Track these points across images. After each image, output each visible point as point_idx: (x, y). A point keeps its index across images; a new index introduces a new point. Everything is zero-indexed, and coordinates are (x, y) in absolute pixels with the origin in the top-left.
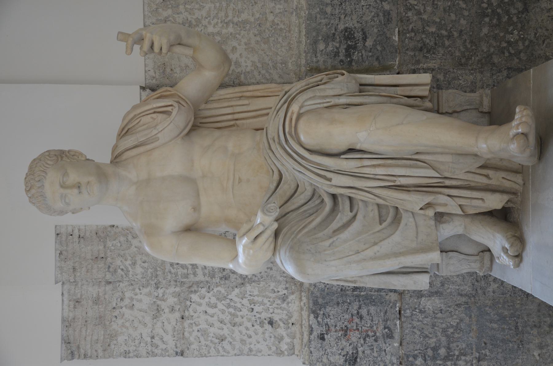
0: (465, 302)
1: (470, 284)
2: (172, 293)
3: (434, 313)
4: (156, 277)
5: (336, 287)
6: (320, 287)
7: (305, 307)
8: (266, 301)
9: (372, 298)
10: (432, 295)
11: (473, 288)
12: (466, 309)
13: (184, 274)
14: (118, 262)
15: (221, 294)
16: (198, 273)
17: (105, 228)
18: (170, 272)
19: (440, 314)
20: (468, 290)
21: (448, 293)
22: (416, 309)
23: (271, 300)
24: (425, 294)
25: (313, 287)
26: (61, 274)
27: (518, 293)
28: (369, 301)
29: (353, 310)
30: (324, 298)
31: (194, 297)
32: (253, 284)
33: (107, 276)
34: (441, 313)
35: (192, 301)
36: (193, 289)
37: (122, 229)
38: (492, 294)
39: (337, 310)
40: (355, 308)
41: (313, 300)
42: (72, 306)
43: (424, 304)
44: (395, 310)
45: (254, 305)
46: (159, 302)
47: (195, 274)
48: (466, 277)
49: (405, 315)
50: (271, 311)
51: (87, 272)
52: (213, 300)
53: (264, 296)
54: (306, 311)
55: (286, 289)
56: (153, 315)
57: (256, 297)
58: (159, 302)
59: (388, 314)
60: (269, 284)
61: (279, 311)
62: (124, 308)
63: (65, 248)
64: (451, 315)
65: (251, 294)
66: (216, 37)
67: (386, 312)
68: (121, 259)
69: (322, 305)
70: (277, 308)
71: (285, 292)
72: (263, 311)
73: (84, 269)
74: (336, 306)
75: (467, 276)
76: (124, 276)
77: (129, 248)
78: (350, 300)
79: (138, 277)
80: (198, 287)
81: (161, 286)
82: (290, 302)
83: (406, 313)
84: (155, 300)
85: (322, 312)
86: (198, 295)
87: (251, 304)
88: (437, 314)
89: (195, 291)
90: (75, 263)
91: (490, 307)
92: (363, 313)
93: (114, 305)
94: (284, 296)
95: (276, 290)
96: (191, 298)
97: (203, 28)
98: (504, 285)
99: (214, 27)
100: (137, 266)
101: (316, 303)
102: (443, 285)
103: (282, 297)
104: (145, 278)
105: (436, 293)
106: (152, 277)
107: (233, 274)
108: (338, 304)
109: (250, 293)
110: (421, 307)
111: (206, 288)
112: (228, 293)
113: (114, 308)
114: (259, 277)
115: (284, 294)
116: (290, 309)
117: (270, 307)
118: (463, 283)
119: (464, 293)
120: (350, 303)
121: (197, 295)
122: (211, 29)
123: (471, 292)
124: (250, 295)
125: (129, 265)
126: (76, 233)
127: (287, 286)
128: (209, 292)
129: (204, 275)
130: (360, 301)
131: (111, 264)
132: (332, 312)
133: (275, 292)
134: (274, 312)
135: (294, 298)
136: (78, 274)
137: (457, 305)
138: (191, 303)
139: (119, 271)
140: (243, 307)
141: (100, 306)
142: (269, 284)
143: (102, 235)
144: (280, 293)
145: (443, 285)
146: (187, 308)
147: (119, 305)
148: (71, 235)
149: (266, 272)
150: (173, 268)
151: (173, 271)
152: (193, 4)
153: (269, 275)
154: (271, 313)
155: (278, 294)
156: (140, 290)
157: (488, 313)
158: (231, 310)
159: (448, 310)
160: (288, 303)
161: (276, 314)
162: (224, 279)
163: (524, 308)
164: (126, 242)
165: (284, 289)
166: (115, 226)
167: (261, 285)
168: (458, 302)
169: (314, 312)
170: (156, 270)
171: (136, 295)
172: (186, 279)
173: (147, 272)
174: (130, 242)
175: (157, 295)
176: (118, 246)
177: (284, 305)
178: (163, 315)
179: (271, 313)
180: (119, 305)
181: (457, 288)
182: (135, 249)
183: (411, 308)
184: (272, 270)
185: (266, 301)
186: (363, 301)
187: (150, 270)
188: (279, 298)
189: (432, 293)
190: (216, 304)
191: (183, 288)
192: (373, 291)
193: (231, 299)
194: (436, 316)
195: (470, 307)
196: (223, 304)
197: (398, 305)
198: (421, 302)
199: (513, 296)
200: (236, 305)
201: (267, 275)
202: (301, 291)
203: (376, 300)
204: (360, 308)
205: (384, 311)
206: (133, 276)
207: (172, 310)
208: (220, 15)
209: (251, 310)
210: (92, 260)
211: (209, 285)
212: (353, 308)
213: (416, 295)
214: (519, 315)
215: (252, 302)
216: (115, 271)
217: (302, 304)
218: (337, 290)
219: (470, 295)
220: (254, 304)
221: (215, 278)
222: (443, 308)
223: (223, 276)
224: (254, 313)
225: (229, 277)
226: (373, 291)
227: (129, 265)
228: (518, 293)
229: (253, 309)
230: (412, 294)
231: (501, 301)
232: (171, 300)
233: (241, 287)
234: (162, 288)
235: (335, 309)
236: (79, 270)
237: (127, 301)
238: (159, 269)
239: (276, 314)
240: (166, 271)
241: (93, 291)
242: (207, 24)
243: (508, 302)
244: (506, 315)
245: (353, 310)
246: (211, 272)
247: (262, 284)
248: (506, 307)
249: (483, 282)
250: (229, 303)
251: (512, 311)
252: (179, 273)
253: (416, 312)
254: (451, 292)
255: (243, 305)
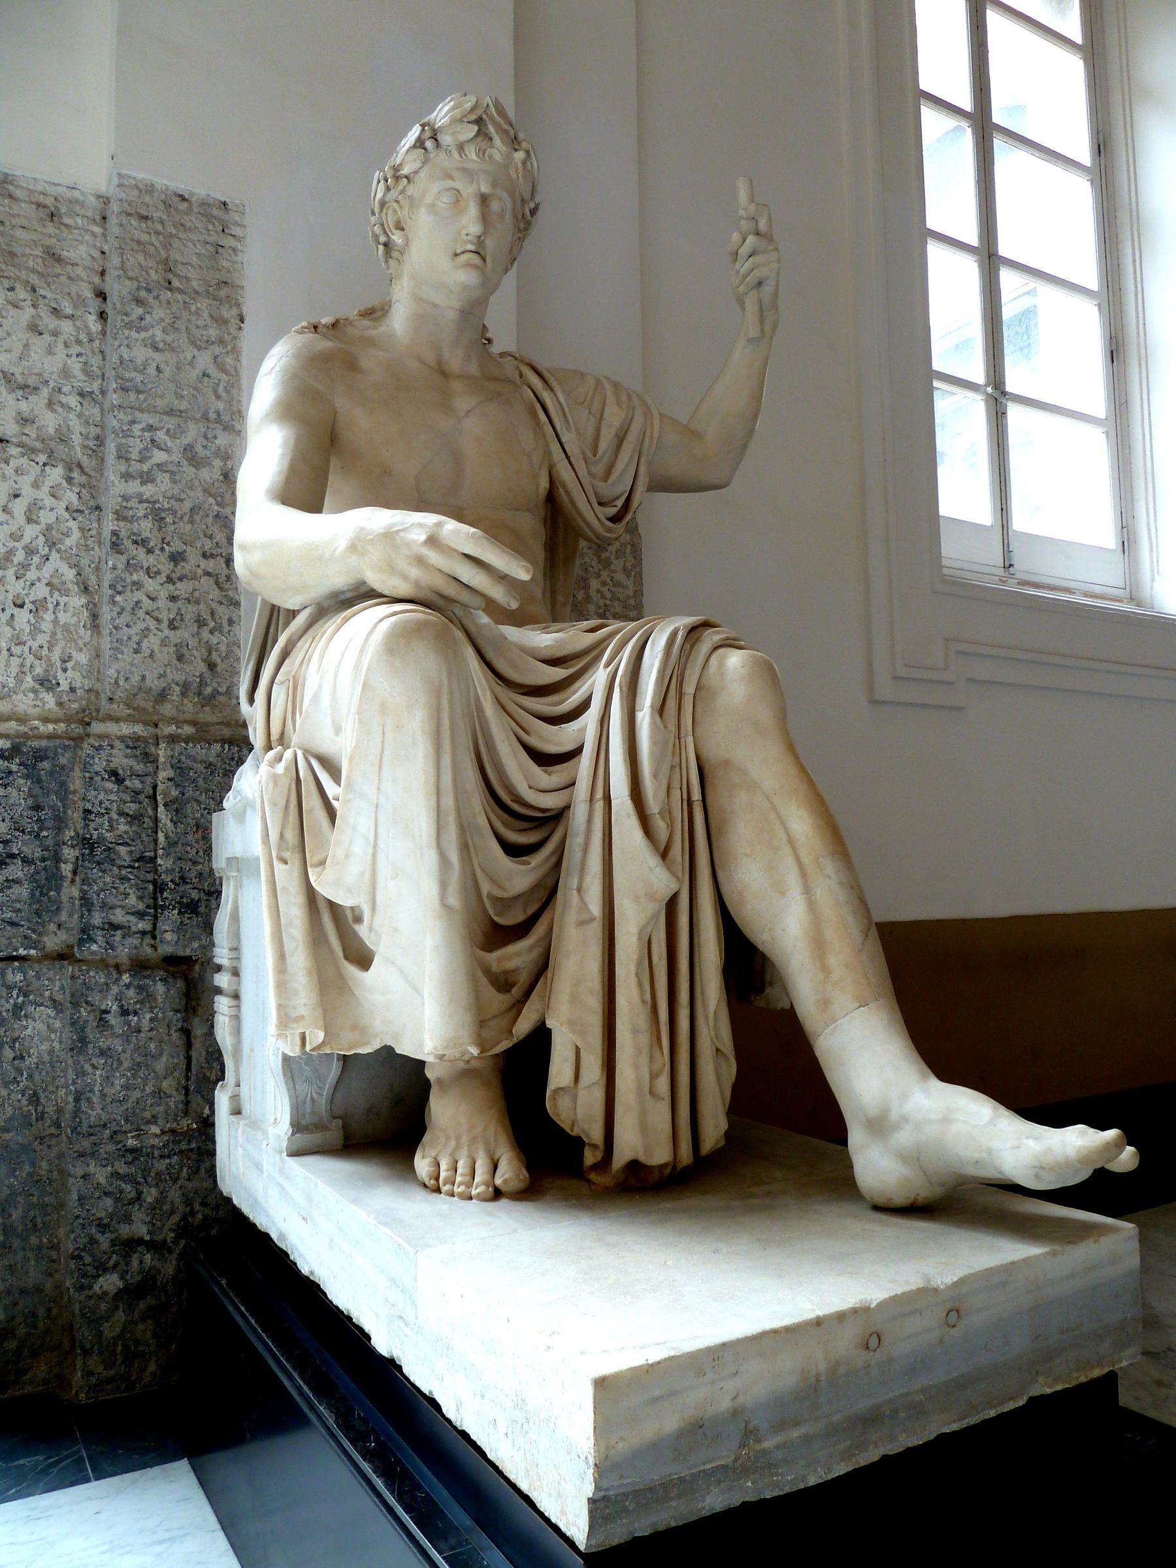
0: (43, 1113)
1: (104, 1117)
2: (68, 426)
3: (15, 1040)
4: (122, 389)
5: (96, 798)
6: (97, 760)
7: (26, 730)
8: (42, 639)
9: (50, 890)
10: (76, 1029)
11: (96, 1126)
12: (25, 1117)
13: (127, 452)
14: (159, 313)
15: (61, 536)
16: (130, 483)
17: (238, 305)
18: (133, 422)
19: (12, 1055)
20: (90, 1115)
21: (82, 1067)
22: (25, 995)
23: (45, 652)
24: (79, 1012)
25: (97, 744)
26: (136, 187)
27: (83, 1235)
28: (44, 882)
29: (20, 843)
30: (51, 773)
31: (56, 474)
32: (86, 614)
33: (128, 282)
34: (14, 1059)
35: (47, 468)
36: (75, 475)
37: (235, 338)
38: (80, 1172)
39: (20, 804)
40: (24, 849)
41: (47, 749)
42: (41, 199)
43: (37, 1015)
44: (19, 945)
45: (31, 611)
46: (45, 392)
47: (127, 476)
48: (125, 1107)
49: (9, 971)
50: (16, 650)
51: (139, 242)
52: (46, 518)
53: (54, 634)
54: (17, 731)
55: (71, 688)
56: (13, 374)
57: (53, 617)
58: (45, 392)
59: (8, 928)
60: (84, 649)
61: (14, 669)
62: (32, 311)
63: (196, 210)
64: (10, 1083)
65: (61, 607)
66: (582, 592)
67: (13, 924)
68: (167, 321)
69: (34, 769)
70: (22, 665)
71: (65, 686)
72: (15, 629)
73: (145, 238)
74: (30, 802)
75: (127, 1110)
76: (127, 319)
77: (192, 342)
78: (47, 837)
79: (124, 349)
80: (82, 486)
81: (85, 404)
82: (37, 696)
83: (13, 973)
84: (52, 384)
85: (14, 768)
86: (60, 484)
87: (33, 602)
88: (12, 1048)
89: (72, 478)
90: (162, 222)
91: (30, 1175)
92: (11, 868)
93: (42, 292)
94: (54, 682)
95: (69, 665)
96: (53, 465)
97: (596, 570)
98: (104, 1198)
99: (598, 591)
100: (150, 353)
101: (39, 755)
102: (103, 1053)
103: (51, 678)
104: (121, 363)
105: (83, 1040)
106: (122, 379)
107: (125, 562)
108: (37, 808)
109: (62, 604)
110: (31, 1009)
111: (77, 503)
112: (66, 551)
113: (34, 290)
114: (117, 621)
115: (58, 684)
116: (20, 696)
117: (26, 649)
118: (109, 1100)
119: (84, 1105)
120: (37, 836)
121: (60, 480)
122: (594, 584)
123: (85, 1124)
124: (58, 604)
125: (154, 335)
126: (228, 242)
127: (79, 692)
128: (67, 509)
129: (125, 498)
130: (43, 860)
131: (157, 297)
132: (15, 793)
133: (64, 661)
134: (11, 655)
135: (47, 707)
136: (133, 222)
137: (35, 1094)
138: (41, 464)
139: (140, 311)
140: (28, 583)
141: (40, 261)
142: (84, 649)
143: (222, 294)
144: (61, 676)
145: (103, 1053)
146: (29, 451)
147: (41, 301)
148: (223, 231)
149: (129, 638)
150: (143, 430)
151: (137, 428)
152: (632, 559)
153: (121, 644)
154: (9, 650)
155: (60, 669)
156: (77, 356)
157: (14, 1172)
158: (20, 556)
159: (22, 1075)
160: (35, 691)
161: (8, 661)
162: (114, 539)
163: (30, 1254)
164: (205, 338)
165: (71, 683)
166: (242, 325)
167: (82, 631)
168: (42, 1095)
169: (16, 750)
170: (139, 392)
171: (65, 343)
172: (114, 451)
173: (135, 370)
174: (206, 348)
175: (64, 390)
176: (197, 320)
177: (29, 682)
178: (13, 395)
179: (9, 650)
180: (41, 301)
181: (96, 1089)
182: (189, 356)
183: (28, 986)
184: (136, 653)
185: (42, 639)
186: (45, 869)
187: (139, 378)
188: (48, 671)
189: (83, 1029)
190: (37, 523)
191: (79, 455)
192: (85, 888)
193: (48, 559)
194: (6, 1046)
195: (31, 1125)
196: (37, 537)
197: (33, 952)
198: (42, 1008)
199: (75, 1224)
200: (33, 567)
201: (122, 640)
202: (68, 720)
203: (45, 899)
204: (26, 861)
205: (15, 920)
206: (127, 338)
207: (24, 420)
208: (616, 603)
209: (19, 602)
210: (167, 259)
211: (86, 512)
212: (23, 845)
213: (77, 990)
214: (10, 1247)
215: (39, 607)
216: (139, 302)
217: (36, 722)
218: (89, 801)
219: (78, 1120)
220: (34, 610)
221: (118, 520)
222: (27, 1063)
223: (122, 540)
224: (11, 609)
225: (118, 553)
226: (85, 888)
227: (154, 335)
228: (83, 1235)
229: (21, 606)
230: (80, 981)
231: (46, 1199)
232: (50, 422)
233: (79, 587)
234: (81, 404)
235: (22, 801)
236: (143, 225)
237: (49, 322)
238: (141, 397)
239: (8, 661)
240: (137, 413)
241: (80, 252)
242: (603, 578)
243: (46, 1214)
244: (10, 1216)
245: (20, 843)
246: (131, 513)
247: (86, 635)
248: (32, 1213)
249: (111, 1147)
250: (38, 553)
251: (20, 1228)
252: (131, 441)
253: (18, 997)
254: (84, 1074)
255: (33, 584)
